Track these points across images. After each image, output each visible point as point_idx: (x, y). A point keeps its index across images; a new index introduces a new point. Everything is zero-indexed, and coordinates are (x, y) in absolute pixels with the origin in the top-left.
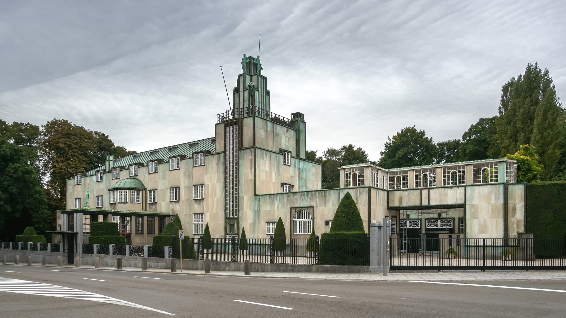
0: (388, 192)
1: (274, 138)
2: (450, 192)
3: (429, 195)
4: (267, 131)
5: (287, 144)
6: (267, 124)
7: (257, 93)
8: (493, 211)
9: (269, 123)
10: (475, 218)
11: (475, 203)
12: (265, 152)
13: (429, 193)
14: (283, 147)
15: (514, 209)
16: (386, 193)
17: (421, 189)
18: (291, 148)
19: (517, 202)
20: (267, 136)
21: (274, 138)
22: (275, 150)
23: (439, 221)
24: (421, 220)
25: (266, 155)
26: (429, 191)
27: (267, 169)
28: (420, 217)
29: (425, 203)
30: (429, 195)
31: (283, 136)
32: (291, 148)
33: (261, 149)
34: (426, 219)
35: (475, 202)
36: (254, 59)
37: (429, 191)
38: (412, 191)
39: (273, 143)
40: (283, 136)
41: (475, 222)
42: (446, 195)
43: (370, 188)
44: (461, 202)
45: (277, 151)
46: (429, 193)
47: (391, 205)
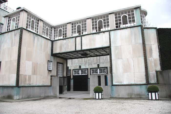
0: (52, 42)
2: (98, 37)
3: (81, 41)
8: (134, 50)
10: (119, 58)
11: (118, 45)
13: (81, 40)
15: (151, 50)
16: (50, 43)
19: (152, 43)
23: (98, 69)
24: (88, 69)
26: (81, 38)
28: (87, 67)
29: (79, 48)
30: (81, 41)
34: (90, 69)
35: (119, 44)
37: (81, 38)
38: (69, 39)
41: (120, 62)
42: (94, 40)
43: (22, 29)
44: (107, 45)
46: (81, 40)
47: (54, 52)
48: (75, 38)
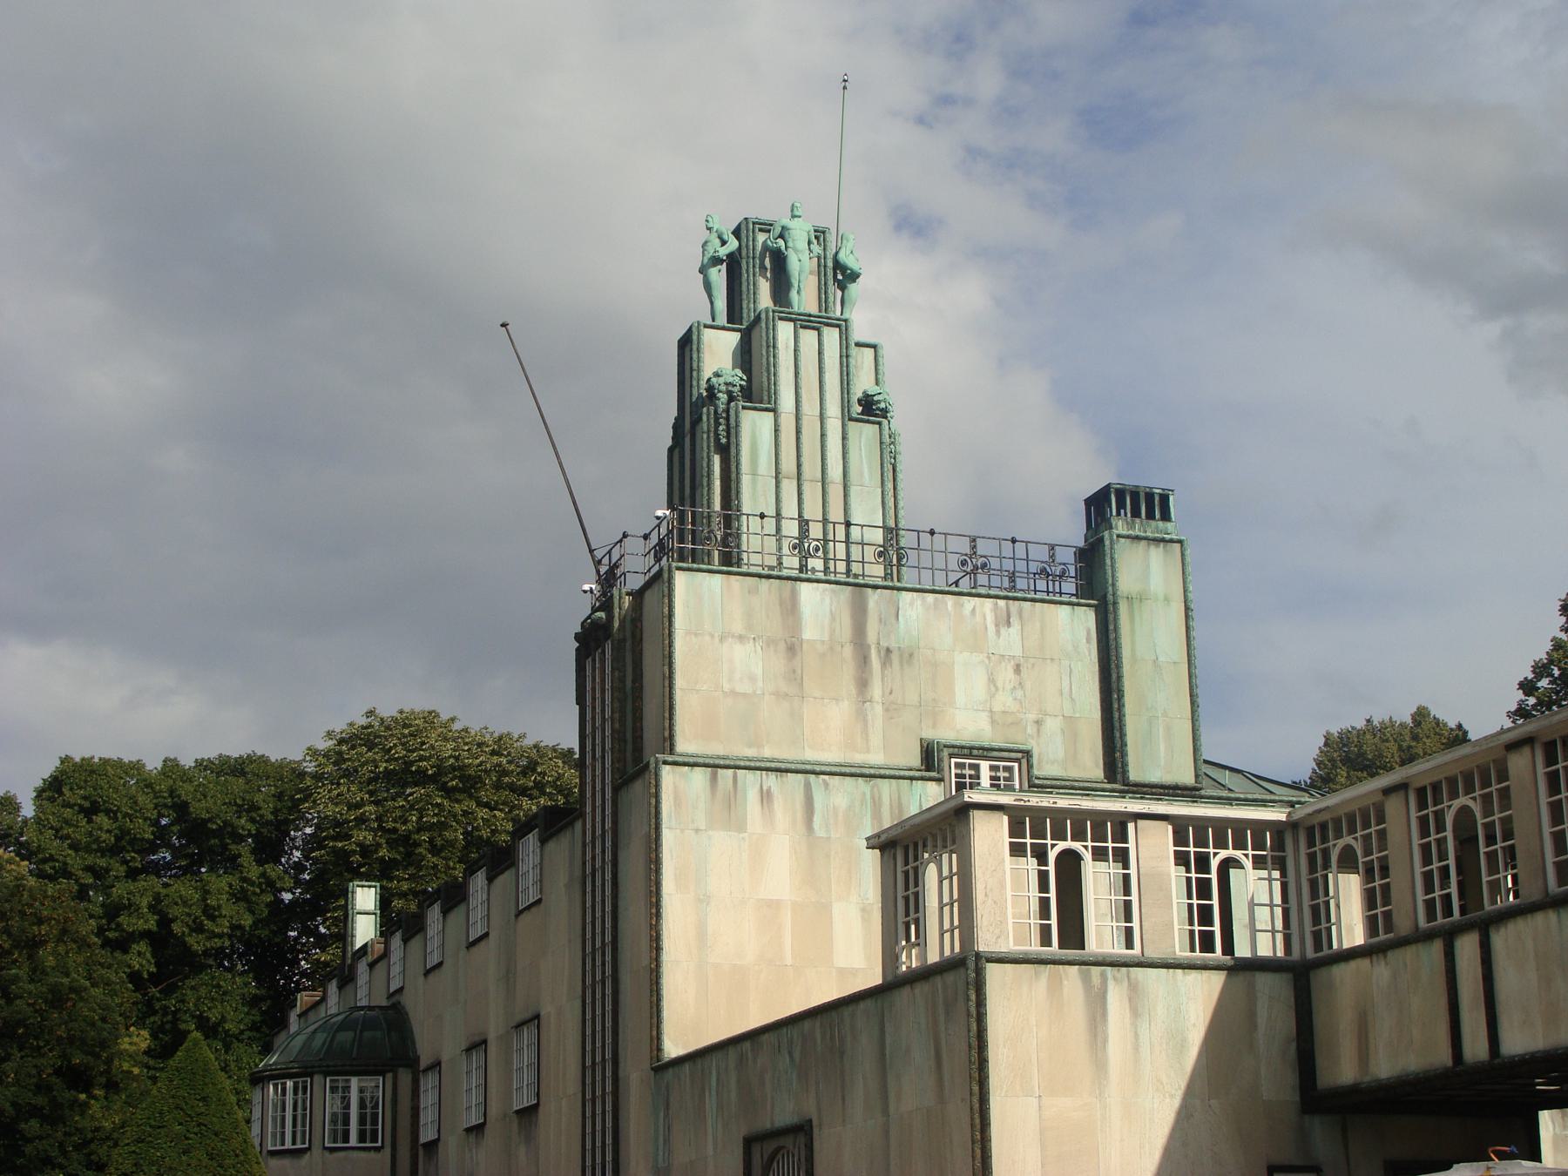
1: (863, 684)
4: (792, 650)
5: (1004, 701)
6: (791, 608)
7: (754, 427)
9: (808, 594)
12: (750, 779)
14: (966, 723)
17: (1449, 936)
18: (1053, 725)
20: (795, 677)
21: (863, 684)
22: (875, 757)
25: (766, 796)
27: (780, 875)
31: (961, 658)
32: (1053, 725)
33: (714, 765)
36: (766, 227)
39: (861, 716)
40: (961, 658)
45: (915, 760)
48: (1437, 947)
